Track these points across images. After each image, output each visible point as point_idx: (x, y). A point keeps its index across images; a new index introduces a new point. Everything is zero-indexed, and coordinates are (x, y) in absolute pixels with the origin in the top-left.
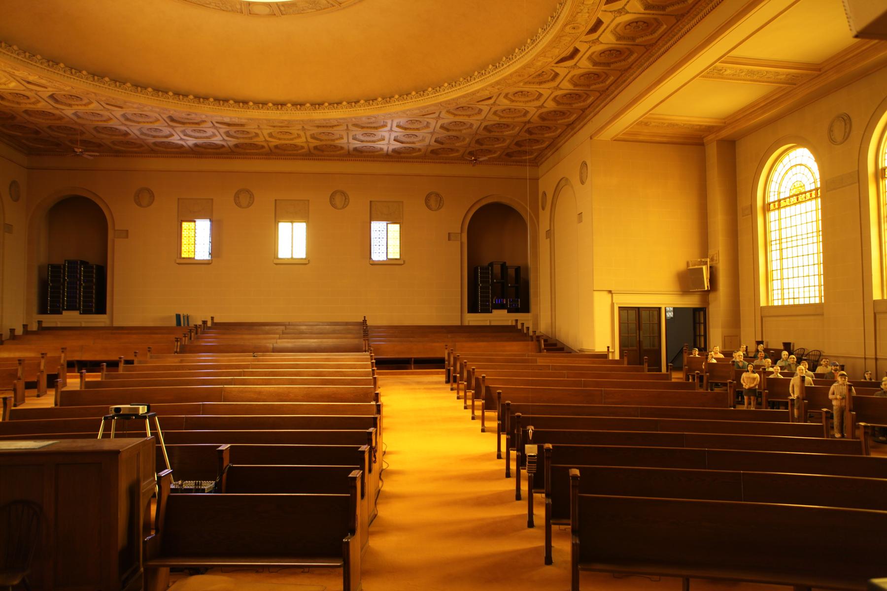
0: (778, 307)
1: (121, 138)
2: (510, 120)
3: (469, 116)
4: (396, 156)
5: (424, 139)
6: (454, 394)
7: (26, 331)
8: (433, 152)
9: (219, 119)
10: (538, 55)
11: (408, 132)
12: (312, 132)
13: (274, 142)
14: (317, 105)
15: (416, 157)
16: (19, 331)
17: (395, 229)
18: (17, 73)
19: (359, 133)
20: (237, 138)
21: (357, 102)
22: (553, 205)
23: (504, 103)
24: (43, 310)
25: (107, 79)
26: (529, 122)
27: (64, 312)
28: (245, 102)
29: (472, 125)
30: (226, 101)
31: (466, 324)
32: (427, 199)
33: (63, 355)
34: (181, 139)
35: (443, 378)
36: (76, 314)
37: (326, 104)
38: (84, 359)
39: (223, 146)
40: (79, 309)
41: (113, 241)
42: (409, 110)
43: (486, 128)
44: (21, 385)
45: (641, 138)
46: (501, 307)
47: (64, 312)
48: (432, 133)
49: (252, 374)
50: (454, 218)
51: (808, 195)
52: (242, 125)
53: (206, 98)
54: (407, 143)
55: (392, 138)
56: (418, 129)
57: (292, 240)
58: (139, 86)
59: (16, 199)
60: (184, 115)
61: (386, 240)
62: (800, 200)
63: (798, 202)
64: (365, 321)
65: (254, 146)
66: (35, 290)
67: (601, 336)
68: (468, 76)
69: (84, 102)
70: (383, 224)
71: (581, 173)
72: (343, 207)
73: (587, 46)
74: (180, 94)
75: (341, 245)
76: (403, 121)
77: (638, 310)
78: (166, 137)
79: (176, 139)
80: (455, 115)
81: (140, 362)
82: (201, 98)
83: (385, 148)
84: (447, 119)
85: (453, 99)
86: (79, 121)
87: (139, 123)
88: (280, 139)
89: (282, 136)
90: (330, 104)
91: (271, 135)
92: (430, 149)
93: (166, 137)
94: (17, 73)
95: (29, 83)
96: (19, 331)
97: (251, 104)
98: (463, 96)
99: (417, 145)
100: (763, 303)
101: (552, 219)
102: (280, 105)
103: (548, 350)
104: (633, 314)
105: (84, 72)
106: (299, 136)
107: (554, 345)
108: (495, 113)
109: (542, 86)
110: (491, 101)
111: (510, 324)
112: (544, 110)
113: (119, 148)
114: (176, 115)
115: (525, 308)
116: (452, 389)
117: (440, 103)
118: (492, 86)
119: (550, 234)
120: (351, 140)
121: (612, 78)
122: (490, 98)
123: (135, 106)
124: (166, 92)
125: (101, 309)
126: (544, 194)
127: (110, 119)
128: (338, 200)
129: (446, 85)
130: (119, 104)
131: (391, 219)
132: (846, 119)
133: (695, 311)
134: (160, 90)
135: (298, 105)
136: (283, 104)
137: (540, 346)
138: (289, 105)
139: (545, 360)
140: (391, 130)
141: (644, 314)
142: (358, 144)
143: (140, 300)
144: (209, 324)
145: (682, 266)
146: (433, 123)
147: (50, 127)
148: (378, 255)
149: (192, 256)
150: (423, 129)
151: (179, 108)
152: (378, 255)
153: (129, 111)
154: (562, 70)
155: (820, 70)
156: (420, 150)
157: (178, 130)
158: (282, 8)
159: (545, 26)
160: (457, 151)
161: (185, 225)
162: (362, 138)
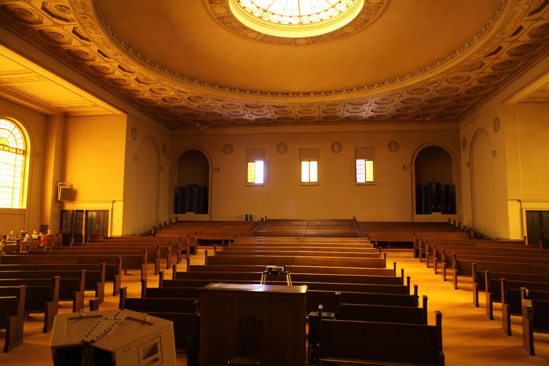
2: (446, 95)
3: (420, 94)
4: (371, 120)
5: (390, 109)
6: (424, 265)
7: (171, 223)
8: (393, 117)
9: (273, 104)
10: (474, 53)
11: (380, 106)
12: (323, 109)
13: (301, 115)
16: (168, 223)
17: (370, 164)
18: (176, 87)
19: (350, 108)
20: (280, 114)
21: (352, 90)
22: (472, 146)
23: (445, 84)
24: (176, 212)
25: (217, 86)
26: (458, 95)
28: (287, 94)
29: (421, 99)
30: (277, 94)
31: (415, 221)
33: (196, 236)
34: (249, 116)
35: (412, 254)
36: (192, 214)
37: (334, 92)
38: (202, 238)
39: (271, 119)
40: (194, 211)
41: (212, 174)
42: (384, 93)
43: (430, 101)
44: (180, 252)
45: (538, 100)
46: (437, 210)
48: (395, 106)
49: (304, 249)
50: (407, 156)
52: (285, 107)
53: (266, 93)
54: (378, 112)
55: (370, 110)
56: (387, 104)
57: (309, 171)
58: (232, 89)
59: (165, 153)
60: (254, 103)
64: (355, 219)
65: (289, 118)
66: (172, 201)
67: (515, 230)
68: (423, 70)
70: (363, 161)
71: (494, 125)
72: (339, 152)
73: (508, 44)
74: (253, 92)
75: (338, 173)
76: (378, 100)
77: (540, 213)
78: (242, 116)
79: (246, 117)
80: (411, 94)
81: (237, 241)
82: (264, 93)
83: (364, 116)
84: (406, 96)
85: (413, 85)
86: (199, 110)
87: (229, 109)
88: (304, 114)
89: (305, 112)
90: (335, 92)
91: (299, 112)
92: (392, 115)
93: (242, 116)
94: (176, 87)
95: (180, 92)
96: (168, 223)
97: (291, 94)
98: (420, 82)
99: (384, 113)
101: (471, 155)
102: (306, 94)
103: (476, 238)
104: (536, 215)
105: (206, 84)
106: (315, 111)
107: (479, 236)
108: (437, 91)
109: (472, 72)
110: (436, 84)
111: (443, 221)
112: (470, 87)
114: (248, 103)
115: (453, 211)
116: (421, 261)
117: (404, 87)
118: (439, 75)
119: (469, 164)
120: (345, 112)
121: (521, 63)
122: (436, 82)
125: (205, 211)
127: (215, 108)
129: (408, 76)
130: (221, 99)
131: (367, 158)
134: (242, 90)
135: (317, 93)
137: (470, 235)
138: (312, 94)
139: (480, 244)
140: (370, 105)
142: (348, 114)
143: (226, 208)
144: (264, 220)
146: (396, 99)
147: (184, 114)
148: (360, 179)
149: (253, 181)
151: (251, 100)
152: (360, 179)
153: (224, 103)
154: (487, 62)
156: (385, 116)
157: (249, 112)
158: (314, 40)
159: (479, 34)
160: (408, 115)
161: (249, 164)
162: (352, 111)
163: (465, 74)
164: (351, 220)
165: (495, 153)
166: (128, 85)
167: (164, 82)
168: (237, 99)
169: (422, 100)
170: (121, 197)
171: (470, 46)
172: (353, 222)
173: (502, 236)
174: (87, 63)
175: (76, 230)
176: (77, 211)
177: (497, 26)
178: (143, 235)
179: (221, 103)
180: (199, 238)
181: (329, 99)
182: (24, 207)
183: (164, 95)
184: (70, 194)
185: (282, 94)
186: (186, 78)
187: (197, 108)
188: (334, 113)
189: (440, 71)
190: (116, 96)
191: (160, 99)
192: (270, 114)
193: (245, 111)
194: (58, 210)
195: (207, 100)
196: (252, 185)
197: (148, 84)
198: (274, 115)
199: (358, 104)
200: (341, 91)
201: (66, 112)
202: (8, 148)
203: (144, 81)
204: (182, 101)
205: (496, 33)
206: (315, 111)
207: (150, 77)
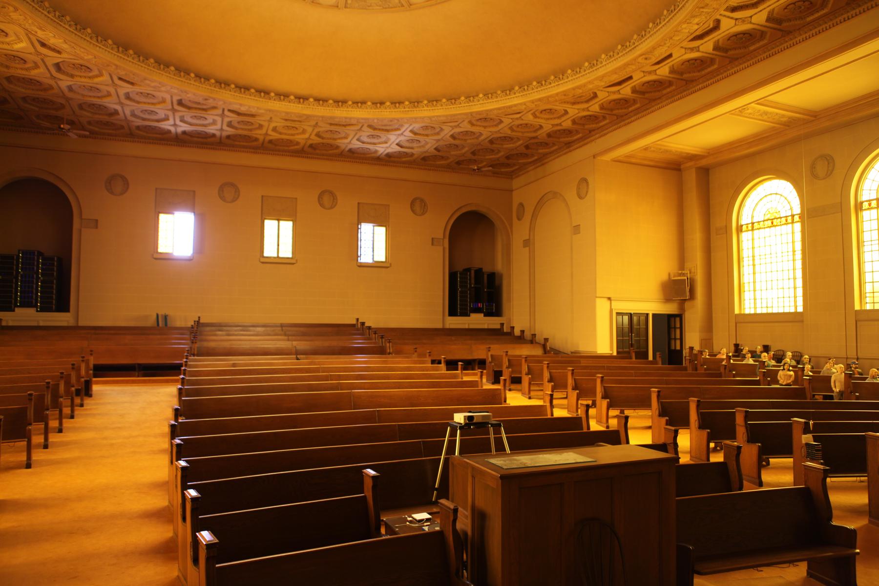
0: (750, 315)
1: (105, 118)
2: (520, 134)
3: (485, 127)
4: (389, 160)
5: (429, 144)
10: (596, 79)
13: (274, 136)
14: (340, 102)
15: (404, 163)
21: (382, 103)
22: (534, 216)
23: (529, 118)
25: (131, 52)
26: (536, 138)
27: (16, 309)
29: (481, 134)
30: (247, 89)
31: (447, 326)
32: (412, 204)
34: (175, 125)
36: (31, 311)
37: (350, 103)
40: (36, 306)
41: (80, 231)
43: (491, 142)
45: (633, 160)
46: (477, 310)
47: (16, 309)
48: (438, 140)
50: (438, 223)
51: (783, 220)
52: (253, 116)
55: (397, 141)
57: (278, 238)
58: (163, 64)
60: (201, 100)
61: (373, 243)
62: (775, 223)
63: (773, 225)
68: (508, 90)
69: (91, 74)
71: (578, 188)
72: (332, 208)
73: (642, 74)
75: (325, 245)
76: (416, 126)
78: (158, 121)
79: (166, 125)
80: (473, 125)
82: (223, 83)
84: (466, 127)
86: (70, 95)
87: (138, 102)
90: (354, 103)
91: (275, 129)
93: (158, 121)
98: (499, 109)
100: (737, 311)
101: (532, 229)
102: (301, 98)
104: (626, 318)
105: (110, 42)
106: (304, 132)
110: (518, 116)
112: (559, 128)
113: (104, 127)
114: (184, 97)
118: (533, 102)
119: (527, 243)
121: (638, 105)
123: (153, 84)
125: (63, 306)
126: (521, 205)
127: (109, 95)
128: (326, 199)
129: (481, 95)
132: (829, 159)
133: (670, 317)
134: (183, 70)
141: (635, 319)
142: (356, 144)
145: (665, 277)
147: (24, 99)
148: (366, 257)
150: (432, 135)
151: (195, 91)
152: (366, 257)
155: (815, 116)
156: (412, 155)
157: (178, 115)
159: (610, 51)
162: (365, 139)
163: (560, 107)
164: (354, 325)
165: (576, 229)
168: (167, 86)
169: (482, 138)
171: (591, 67)
172: (359, 329)
173: (585, 348)
177: (645, 46)
179: (128, 88)
181: (341, 113)
185: (257, 91)
186: (68, 18)
187: (66, 90)
188: (335, 139)
189: (537, 96)
192: (218, 127)
193: (170, 114)
195: (101, 75)
196: (166, 258)
198: (225, 127)
199: (383, 130)
200: (364, 103)
205: (641, 55)
206: (304, 132)
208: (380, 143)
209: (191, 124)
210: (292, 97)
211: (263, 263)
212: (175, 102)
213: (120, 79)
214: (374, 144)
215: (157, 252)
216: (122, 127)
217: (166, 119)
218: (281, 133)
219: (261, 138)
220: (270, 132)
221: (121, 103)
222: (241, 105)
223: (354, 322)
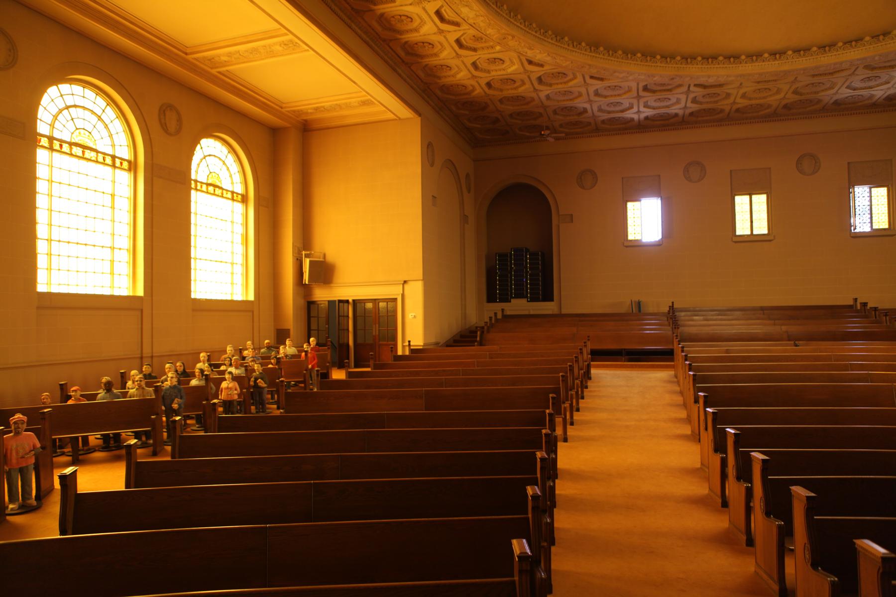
7: (497, 320)
13: (742, 103)
17: (881, 194)
24: (491, 299)
25: (601, 49)
30: (714, 58)
34: (639, 112)
37: (840, 44)
40: (527, 297)
52: (720, 86)
57: (752, 214)
58: (630, 53)
66: (484, 280)
70: (866, 188)
78: (622, 111)
79: (630, 114)
82: (689, 58)
87: (606, 97)
90: (845, 43)
91: (744, 96)
93: (622, 111)
94: (530, 54)
95: (530, 62)
97: (743, 57)
102: (776, 54)
106: (779, 91)
113: (577, 126)
123: (622, 75)
124: (653, 56)
127: (580, 95)
131: (874, 182)
134: (649, 55)
136: (807, 49)
142: (845, 93)
148: (861, 225)
149: (638, 237)
151: (660, 72)
152: (861, 225)
164: (850, 307)
166: (436, 55)
167: (512, 43)
170: (418, 272)
172: (861, 311)
174: (376, 8)
175: (353, 335)
176: (340, 301)
178: (448, 344)
179: (598, 85)
180: (594, 348)
182: (251, 297)
183: (497, 72)
184: (324, 272)
190: (405, 80)
191: (483, 82)
193: (635, 102)
194: (302, 302)
195: (575, 78)
196: (637, 245)
197: (475, 50)
198: (689, 104)
201: (306, 121)
202: (220, 191)
203: (471, 44)
204: (523, 83)
206: (779, 91)
207: (490, 31)
208: (878, 85)
209: (654, 108)
210: (766, 55)
211: (736, 242)
212: (641, 89)
213: (592, 77)
214: (871, 88)
215: (628, 240)
216: (589, 124)
217: (631, 107)
218: (750, 99)
219: (727, 109)
220: (739, 100)
221: (590, 101)
222: (709, 77)
223: (851, 303)
